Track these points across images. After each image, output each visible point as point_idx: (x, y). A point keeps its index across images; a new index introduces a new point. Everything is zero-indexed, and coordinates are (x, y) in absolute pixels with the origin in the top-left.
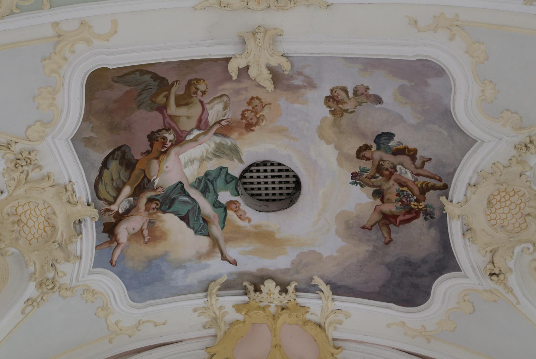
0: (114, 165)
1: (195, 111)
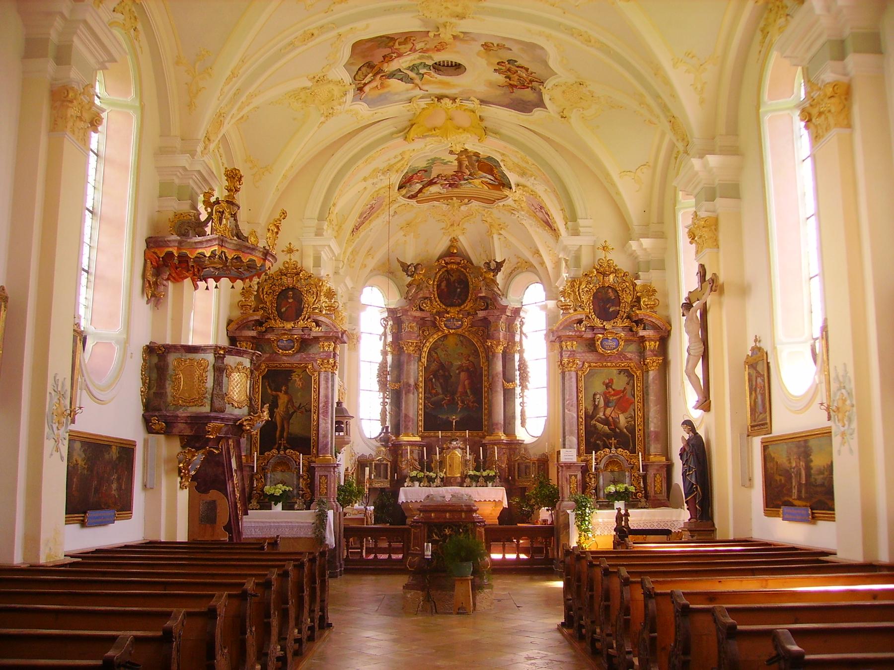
0: (364, 69)
1: (409, 46)
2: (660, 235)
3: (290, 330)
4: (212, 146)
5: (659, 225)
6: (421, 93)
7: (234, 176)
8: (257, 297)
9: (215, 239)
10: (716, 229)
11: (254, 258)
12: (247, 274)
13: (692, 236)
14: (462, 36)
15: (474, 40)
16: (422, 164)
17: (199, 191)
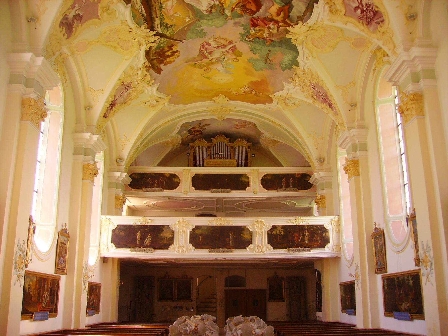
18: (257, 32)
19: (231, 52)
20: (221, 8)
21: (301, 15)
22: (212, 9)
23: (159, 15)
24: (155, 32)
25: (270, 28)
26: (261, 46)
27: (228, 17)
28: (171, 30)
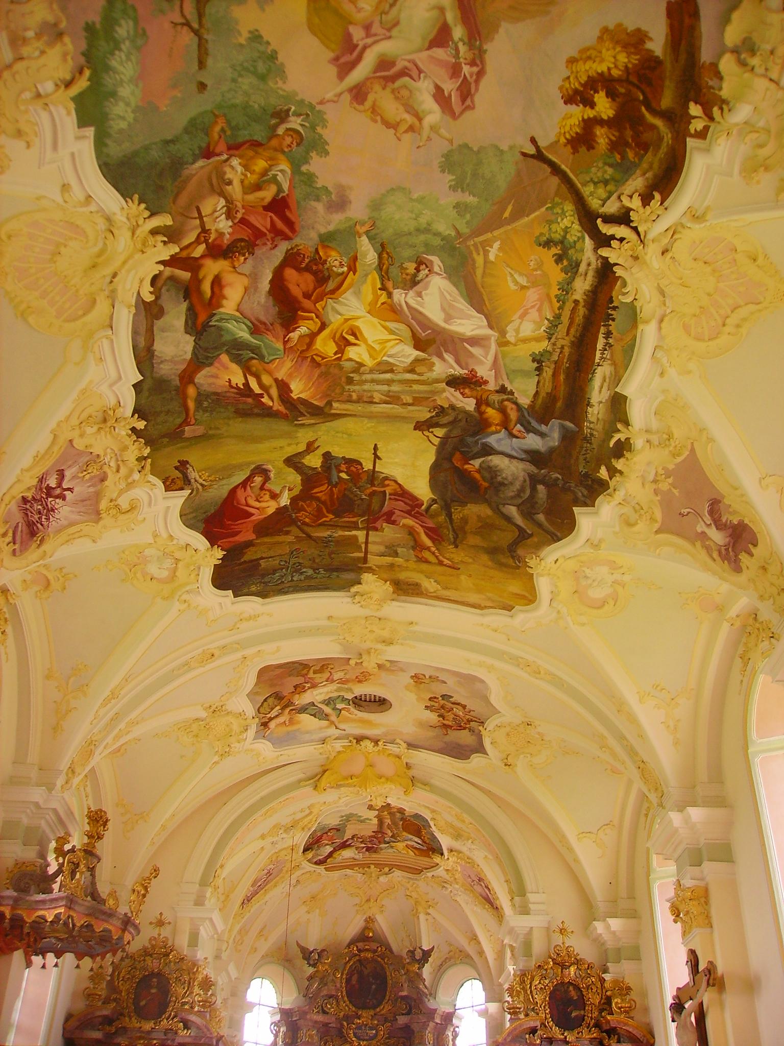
0: (270, 700)
1: (327, 675)
2: (632, 914)
3: (149, 1032)
4: (76, 781)
5: (630, 902)
6: (337, 733)
7: (98, 819)
8: (110, 983)
9: (62, 898)
10: (707, 903)
11: (110, 927)
12: (99, 949)
13: (676, 912)
14: (388, 664)
15: (402, 670)
16: (334, 821)
17: (52, 836)
18: (265, 173)
19: (357, 34)
20: (387, 272)
21: (158, 324)
22: (415, 276)
23: (569, 306)
24: (604, 252)
25: (229, 215)
26: (239, 100)
27: (367, 233)
28: (554, 227)
